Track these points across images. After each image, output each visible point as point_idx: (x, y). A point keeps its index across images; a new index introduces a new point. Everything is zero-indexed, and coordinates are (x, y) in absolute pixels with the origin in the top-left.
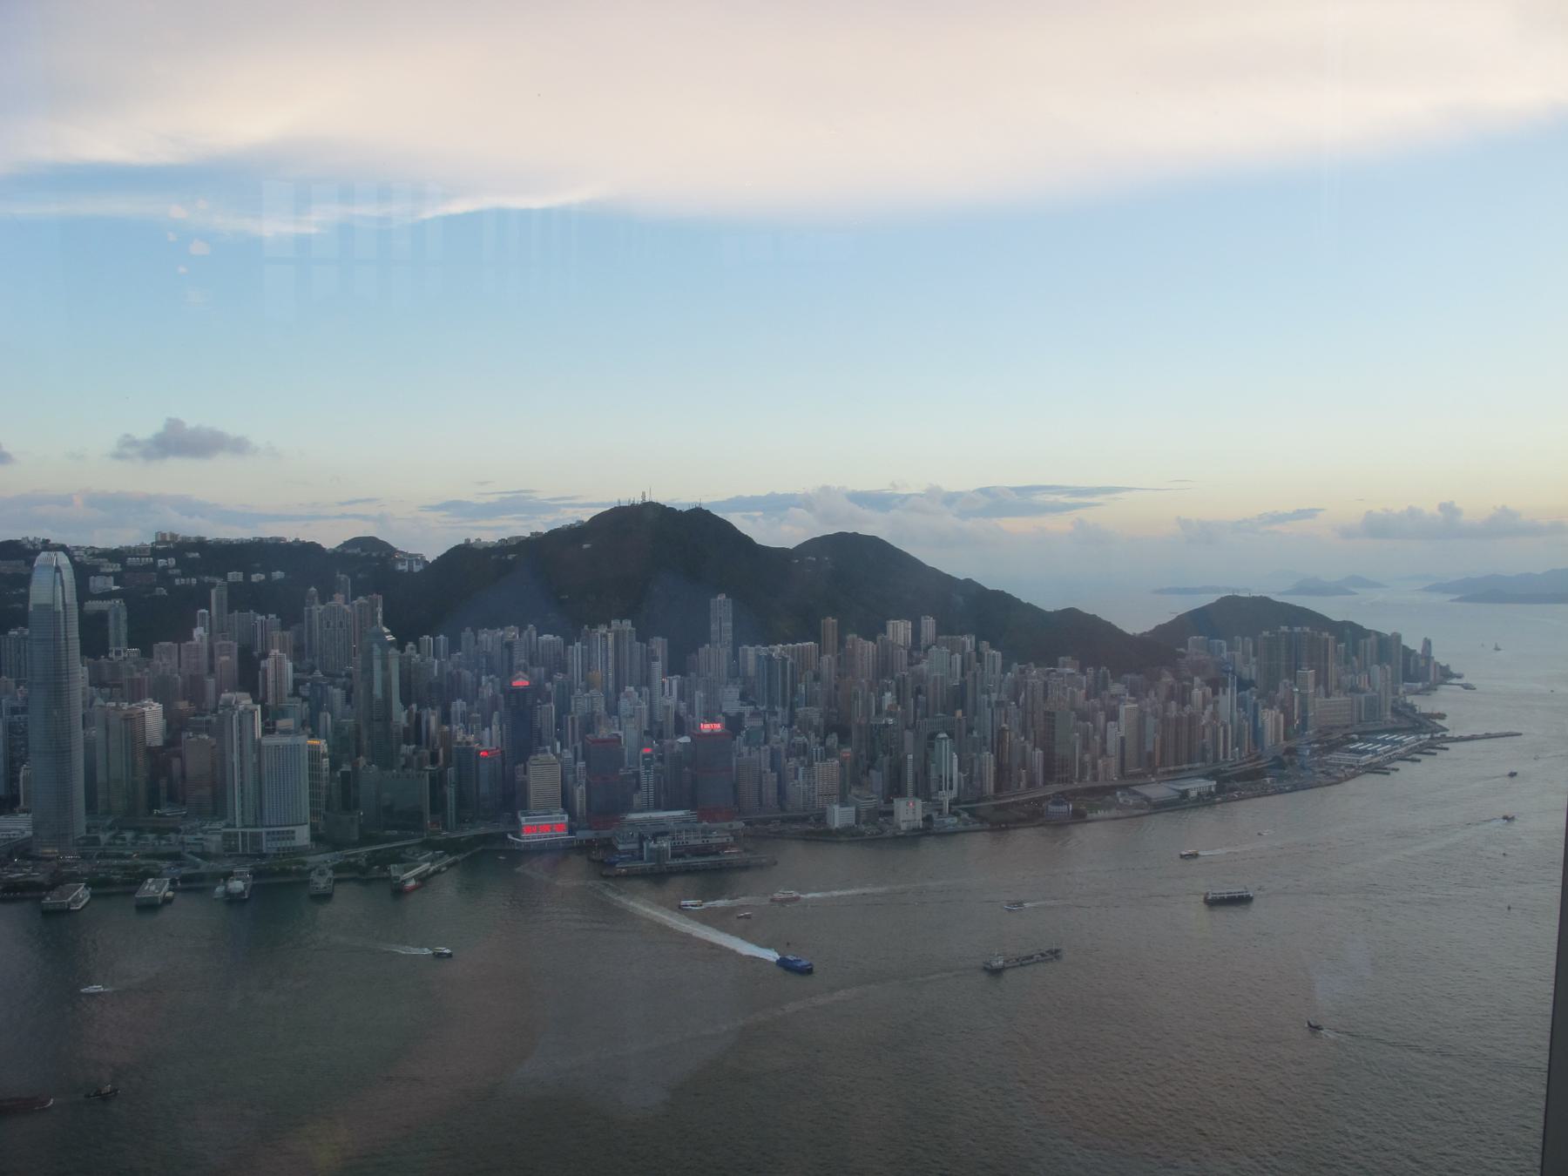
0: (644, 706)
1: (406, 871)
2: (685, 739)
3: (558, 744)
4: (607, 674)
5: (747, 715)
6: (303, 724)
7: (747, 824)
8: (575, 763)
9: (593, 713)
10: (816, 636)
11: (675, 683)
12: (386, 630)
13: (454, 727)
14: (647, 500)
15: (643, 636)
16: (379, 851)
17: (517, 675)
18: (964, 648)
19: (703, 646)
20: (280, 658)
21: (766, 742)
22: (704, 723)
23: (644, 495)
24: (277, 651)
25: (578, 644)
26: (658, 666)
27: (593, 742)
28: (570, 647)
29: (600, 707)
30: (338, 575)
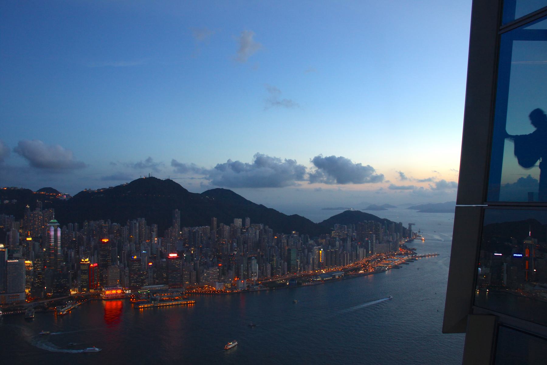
0: (149, 248)
2: (165, 260)
3: (119, 262)
4: (136, 236)
6: (23, 255)
8: (125, 269)
10: (210, 223)
11: (160, 240)
12: (56, 221)
13: (80, 256)
14: (151, 176)
15: (149, 223)
18: (259, 229)
19: (170, 227)
20: (15, 231)
21: (192, 260)
22: (171, 254)
23: (149, 175)
24: (14, 229)
25: (126, 226)
26: (154, 234)
29: (134, 249)
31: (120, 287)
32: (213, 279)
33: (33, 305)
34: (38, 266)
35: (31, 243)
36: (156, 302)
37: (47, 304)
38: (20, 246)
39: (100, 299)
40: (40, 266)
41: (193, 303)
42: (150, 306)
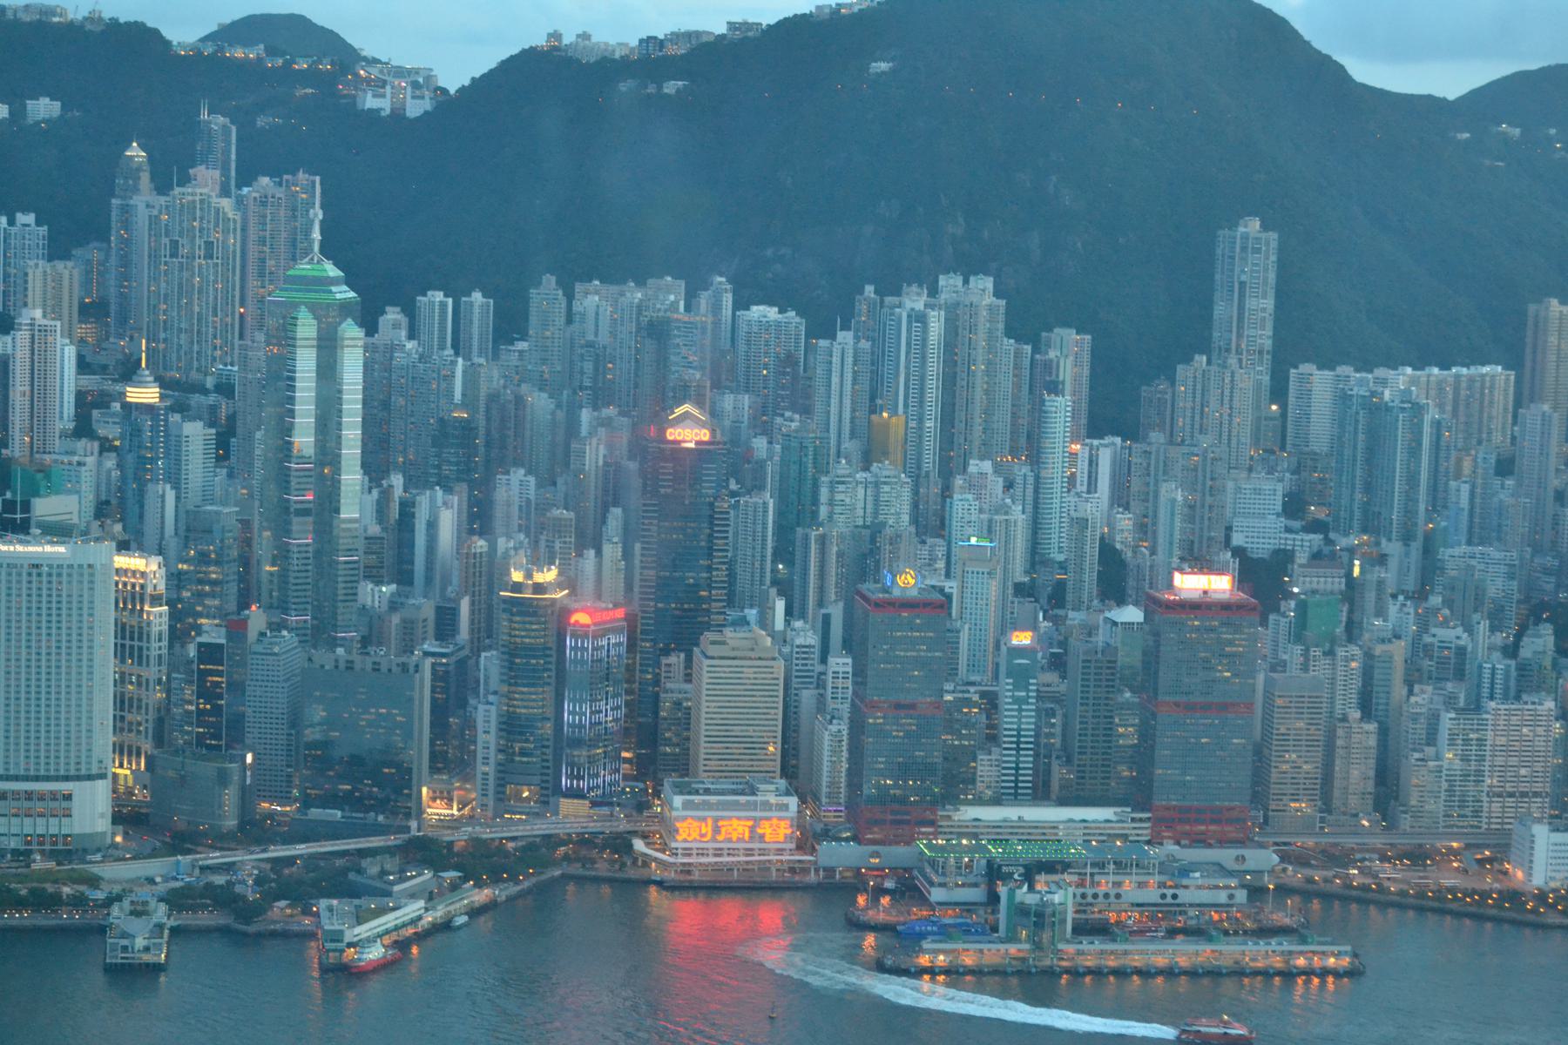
0: (1019, 515)
1: (360, 918)
2: (1132, 614)
3: (780, 605)
4: (921, 420)
5: (1302, 558)
6: (102, 510)
7: (1285, 858)
8: (824, 660)
9: (876, 529)
12: (332, 270)
13: (502, 543)
16: (290, 861)
17: (679, 411)
19: (1188, 360)
20: (44, 330)
21: (1352, 631)
22: (1182, 571)
24: (38, 313)
26: (1061, 409)
27: (880, 605)
28: (823, 343)
29: (899, 514)
30: (204, 116)
31: (779, 793)
32: (1511, 795)
33: (158, 879)
34: (201, 595)
35: (154, 429)
36: (1046, 936)
37: (259, 881)
38: (82, 444)
39: (632, 873)
40: (213, 595)
41: (1337, 974)
42: (996, 960)
